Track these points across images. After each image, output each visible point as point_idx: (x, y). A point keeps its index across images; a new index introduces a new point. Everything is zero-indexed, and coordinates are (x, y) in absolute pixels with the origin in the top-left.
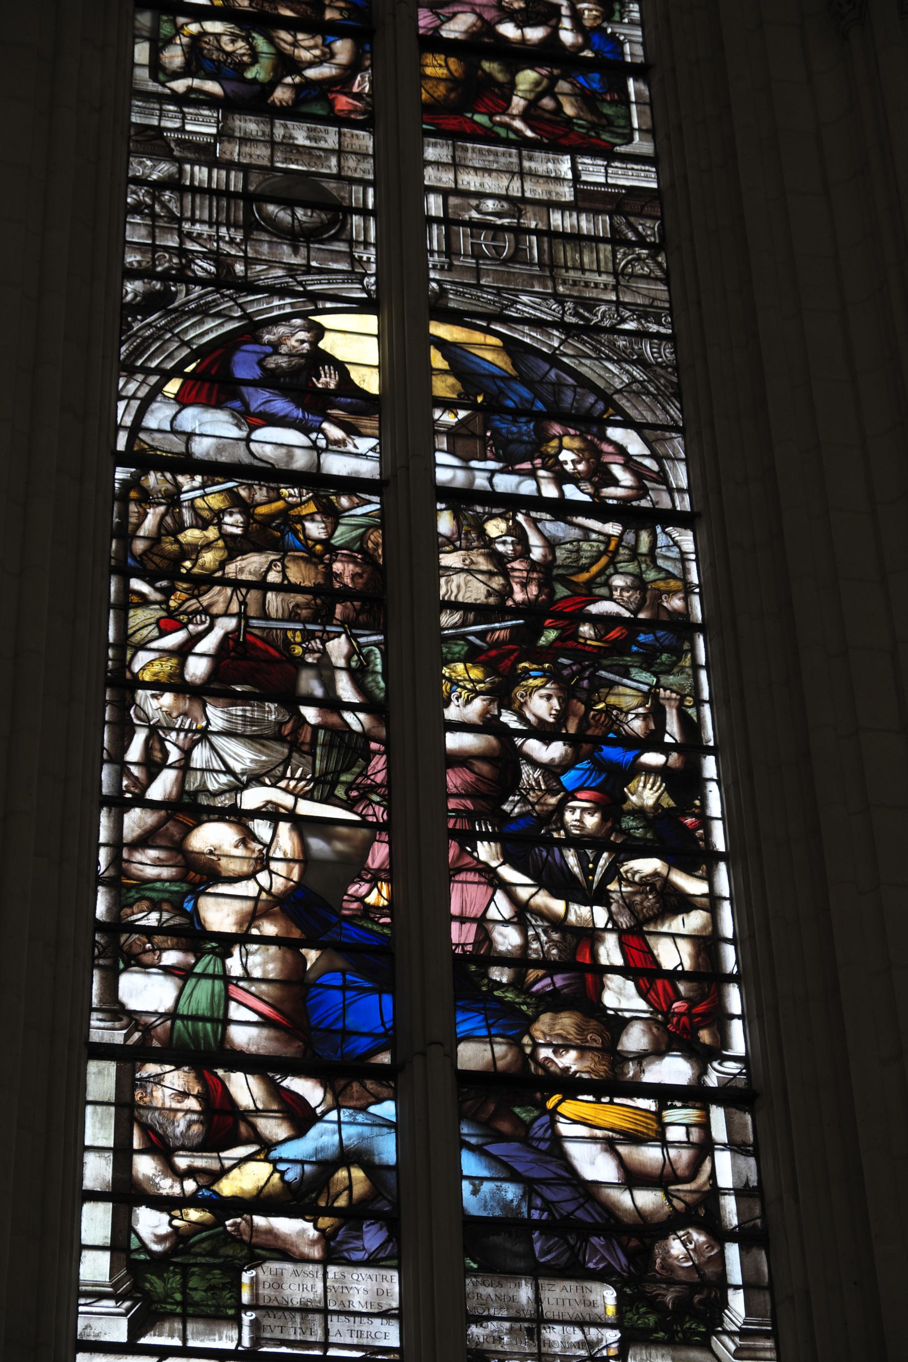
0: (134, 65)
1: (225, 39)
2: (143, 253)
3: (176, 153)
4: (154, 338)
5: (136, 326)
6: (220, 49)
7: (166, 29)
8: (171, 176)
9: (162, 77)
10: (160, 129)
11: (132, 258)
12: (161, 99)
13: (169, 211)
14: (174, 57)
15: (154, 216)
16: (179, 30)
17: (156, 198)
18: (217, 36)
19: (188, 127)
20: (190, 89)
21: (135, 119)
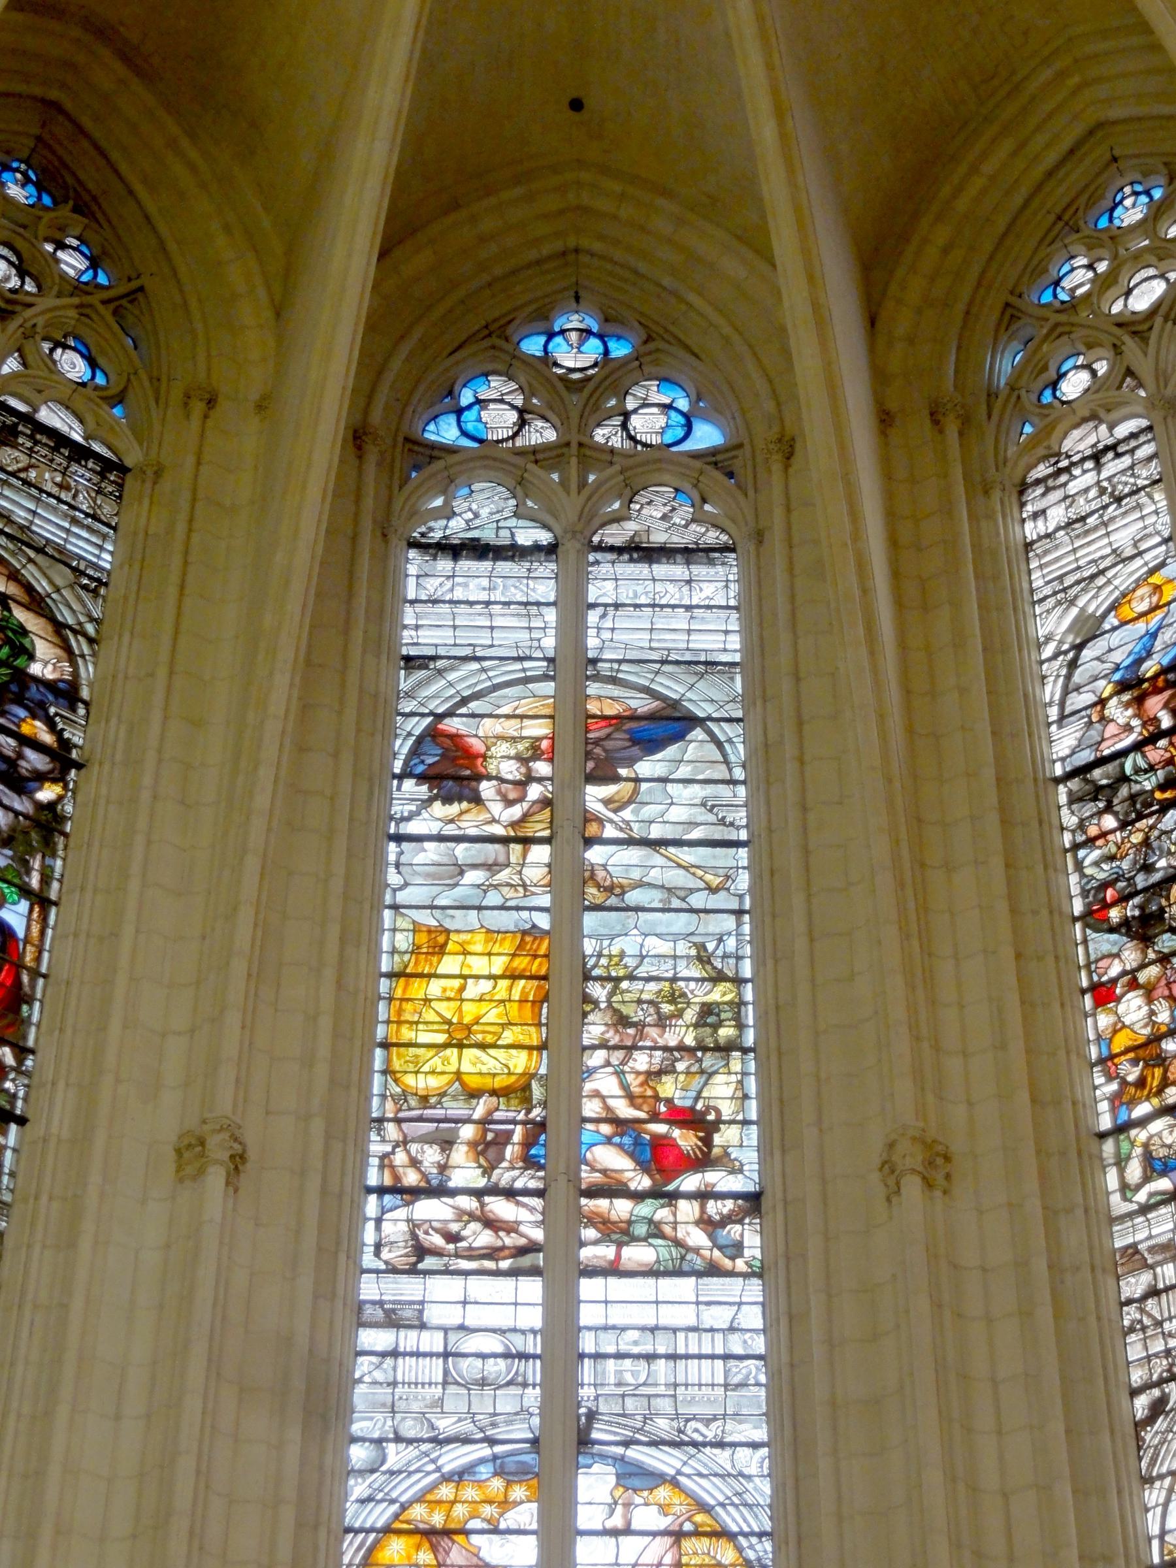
0: (1108, 1194)
1: (1165, 1133)
2: (1142, 1366)
3: (1150, 1261)
4: (1162, 1443)
5: (1148, 1438)
6: (1164, 1145)
7: (1125, 1146)
8: (1149, 1285)
9: (1129, 1195)
10: (1134, 1246)
11: (1137, 1376)
12: (1130, 1215)
13: (1154, 1318)
14: (1134, 1171)
15: (1144, 1329)
16: (1132, 1144)
17: (1142, 1311)
18: (1159, 1135)
19: (1154, 1232)
20: (1151, 1195)
21: (1118, 1244)
